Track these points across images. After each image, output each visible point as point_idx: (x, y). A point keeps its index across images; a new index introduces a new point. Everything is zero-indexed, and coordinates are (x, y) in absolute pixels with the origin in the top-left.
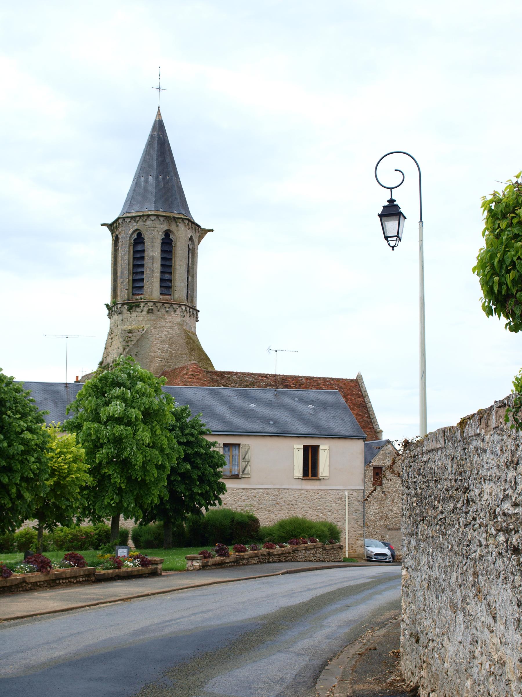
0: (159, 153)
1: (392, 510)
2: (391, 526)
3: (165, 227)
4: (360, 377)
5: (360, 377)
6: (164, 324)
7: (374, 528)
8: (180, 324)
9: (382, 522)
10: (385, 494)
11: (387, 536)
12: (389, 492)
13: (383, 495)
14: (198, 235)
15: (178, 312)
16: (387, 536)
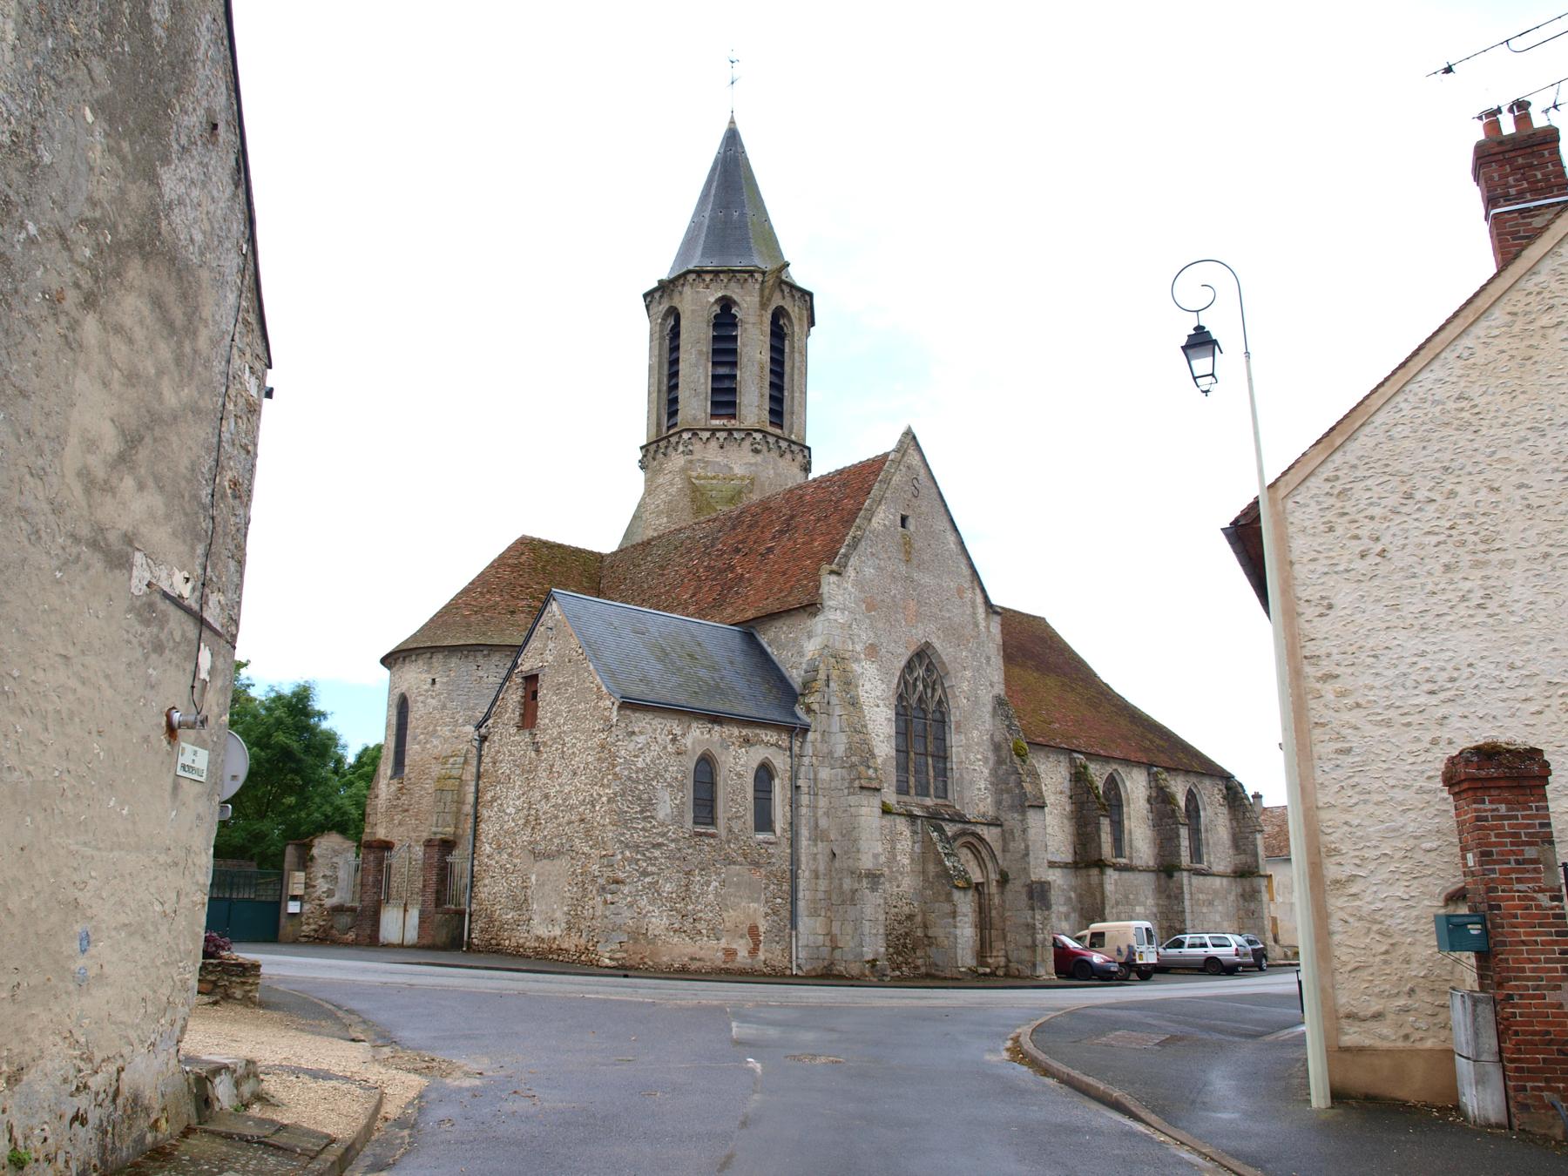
0: (731, 178)
1: (547, 797)
2: (541, 847)
3: (664, 307)
4: (909, 440)
5: (909, 440)
6: (661, 481)
7: (510, 855)
8: (683, 470)
9: (525, 837)
10: (537, 751)
11: (533, 878)
12: (545, 744)
13: (533, 754)
14: (757, 286)
15: (681, 448)
16: (533, 878)
